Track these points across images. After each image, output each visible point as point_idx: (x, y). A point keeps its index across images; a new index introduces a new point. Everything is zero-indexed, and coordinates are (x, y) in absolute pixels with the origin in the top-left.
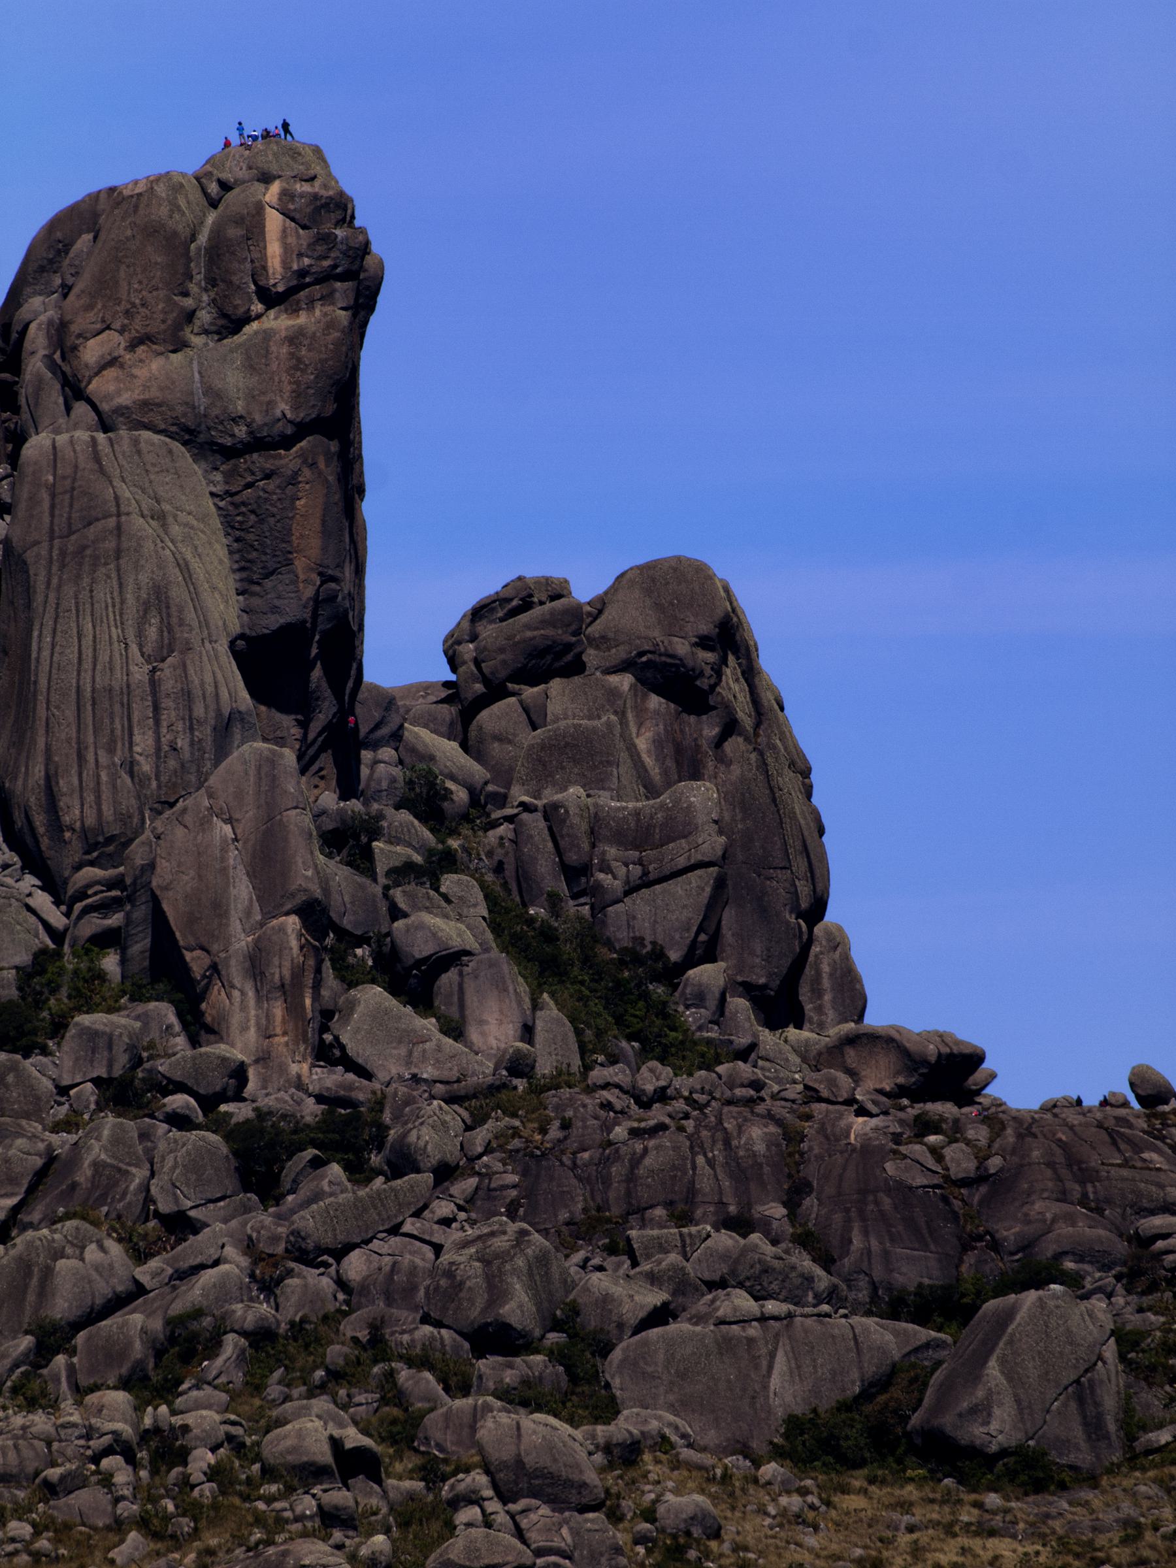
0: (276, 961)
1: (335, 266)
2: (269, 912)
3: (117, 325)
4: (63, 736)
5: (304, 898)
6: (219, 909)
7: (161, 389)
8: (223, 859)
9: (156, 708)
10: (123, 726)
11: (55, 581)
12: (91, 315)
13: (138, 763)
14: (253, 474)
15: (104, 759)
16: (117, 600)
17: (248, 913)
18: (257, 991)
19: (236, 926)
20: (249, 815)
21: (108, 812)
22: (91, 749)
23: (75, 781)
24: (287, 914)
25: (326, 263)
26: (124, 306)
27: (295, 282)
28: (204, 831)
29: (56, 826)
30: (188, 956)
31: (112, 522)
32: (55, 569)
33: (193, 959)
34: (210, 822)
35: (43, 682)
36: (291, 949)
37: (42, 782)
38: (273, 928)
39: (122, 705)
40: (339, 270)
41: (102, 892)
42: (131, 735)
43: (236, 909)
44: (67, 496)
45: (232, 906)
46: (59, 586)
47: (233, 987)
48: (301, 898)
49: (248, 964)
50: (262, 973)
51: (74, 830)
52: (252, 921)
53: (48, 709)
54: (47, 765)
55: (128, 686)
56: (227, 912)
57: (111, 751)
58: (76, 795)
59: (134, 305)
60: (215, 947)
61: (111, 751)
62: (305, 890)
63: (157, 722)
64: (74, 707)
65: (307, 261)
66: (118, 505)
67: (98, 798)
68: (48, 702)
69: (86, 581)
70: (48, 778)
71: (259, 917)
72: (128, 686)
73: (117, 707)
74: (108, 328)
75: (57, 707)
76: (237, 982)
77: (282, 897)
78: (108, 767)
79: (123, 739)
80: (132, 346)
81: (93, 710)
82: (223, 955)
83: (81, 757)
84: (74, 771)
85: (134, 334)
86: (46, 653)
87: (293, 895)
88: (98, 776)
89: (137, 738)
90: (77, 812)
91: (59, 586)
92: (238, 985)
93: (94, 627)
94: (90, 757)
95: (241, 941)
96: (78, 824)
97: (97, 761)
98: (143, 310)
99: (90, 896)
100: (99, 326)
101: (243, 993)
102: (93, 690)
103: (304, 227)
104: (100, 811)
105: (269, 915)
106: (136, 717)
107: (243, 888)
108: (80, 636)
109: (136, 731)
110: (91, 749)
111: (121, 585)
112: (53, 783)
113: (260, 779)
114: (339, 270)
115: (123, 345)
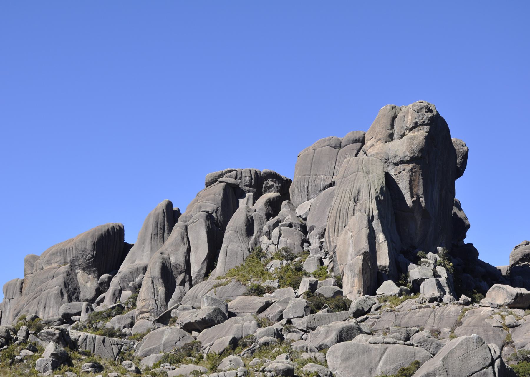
1: (424, 122)
6: (346, 255)
11: (341, 186)
24: (360, 255)
69: (346, 186)
74: (372, 138)
80: (377, 141)
100: (371, 138)
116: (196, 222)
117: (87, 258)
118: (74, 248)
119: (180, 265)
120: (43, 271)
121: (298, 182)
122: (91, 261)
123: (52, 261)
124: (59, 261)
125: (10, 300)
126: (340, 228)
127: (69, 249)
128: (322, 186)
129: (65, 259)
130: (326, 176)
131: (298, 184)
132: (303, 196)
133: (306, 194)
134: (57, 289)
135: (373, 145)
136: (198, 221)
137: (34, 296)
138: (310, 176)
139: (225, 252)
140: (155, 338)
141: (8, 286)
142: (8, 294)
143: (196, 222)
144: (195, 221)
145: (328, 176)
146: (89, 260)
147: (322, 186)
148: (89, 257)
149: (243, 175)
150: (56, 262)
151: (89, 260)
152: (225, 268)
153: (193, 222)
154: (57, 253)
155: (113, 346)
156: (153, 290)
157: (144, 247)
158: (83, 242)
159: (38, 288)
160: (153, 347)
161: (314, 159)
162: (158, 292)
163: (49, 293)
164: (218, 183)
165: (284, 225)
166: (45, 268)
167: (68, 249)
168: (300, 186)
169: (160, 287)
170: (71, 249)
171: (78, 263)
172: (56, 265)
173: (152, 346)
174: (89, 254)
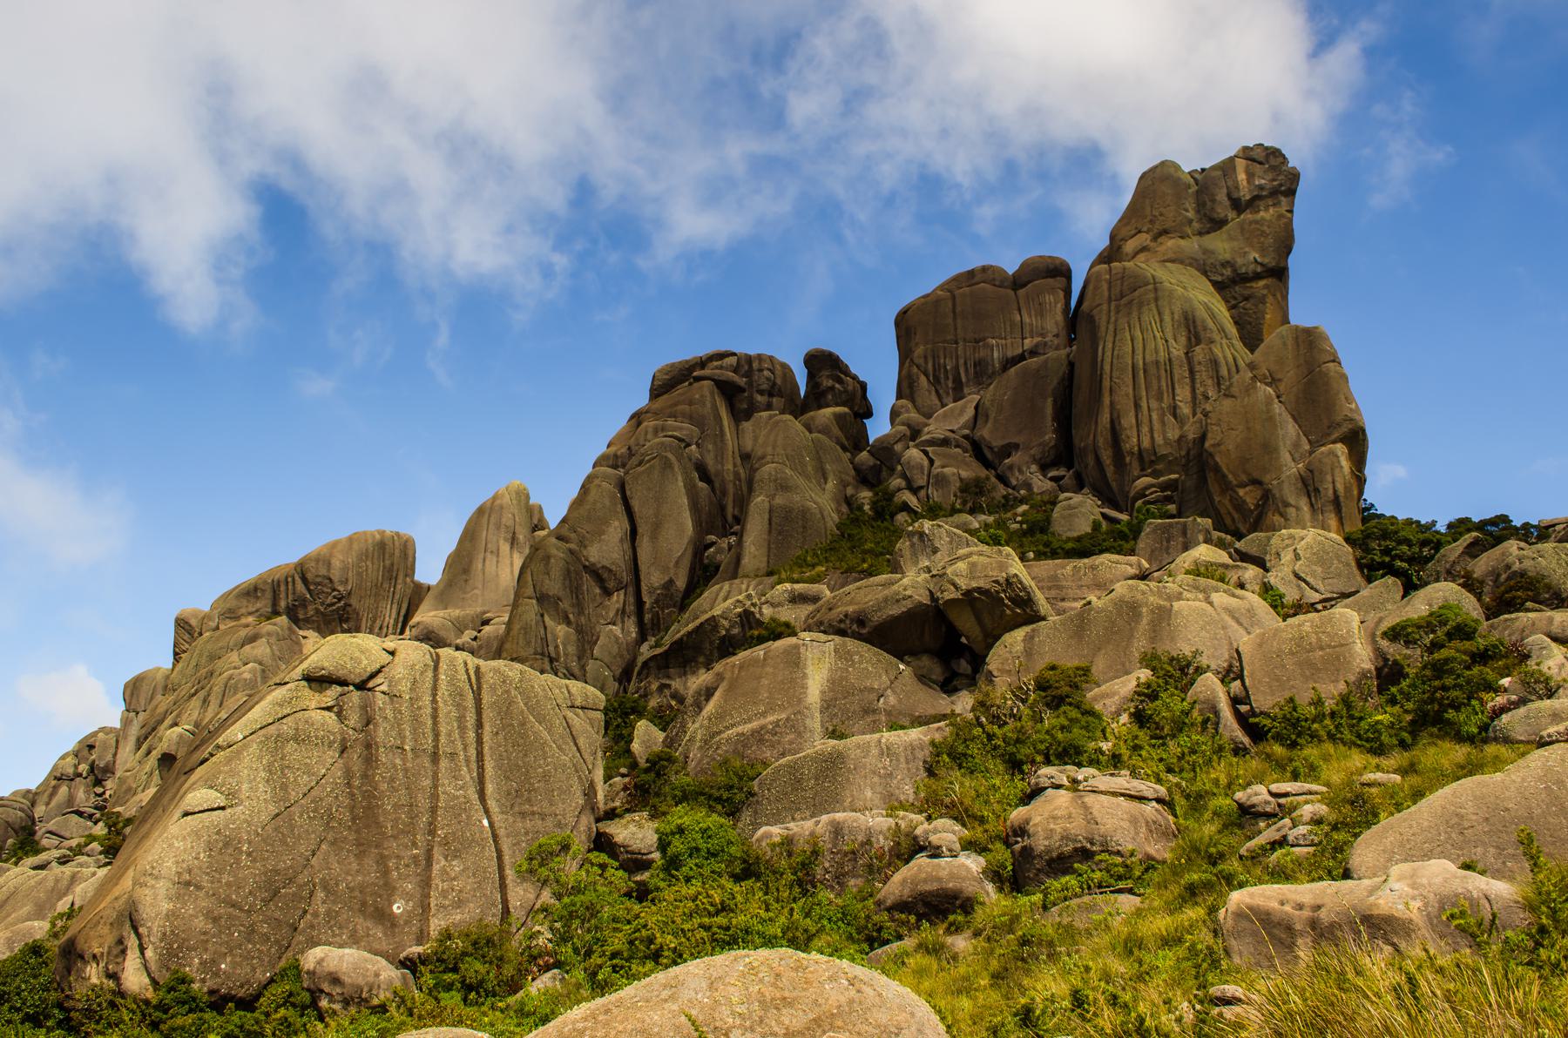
0: (1329, 478)
1: (1281, 185)
2: (1317, 441)
3: (1145, 229)
4: (1123, 393)
5: (1350, 426)
6: (1269, 449)
7: (1175, 253)
8: (1268, 411)
9: (1192, 372)
10: (1167, 386)
11: (1113, 319)
12: (1129, 228)
13: (1180, 408)
14: (1235, 299)
15: (1154, 404)
16: (1158, 320)
17: (1297, 445)
18: (1312, 505)
19: (1286, 457)
20: (1290, 376)
21: (1159, 440)
22: (1144, 399)
23: (1134, 421)
24: (1334, 442)
25: (1275, 183)
26: (1149, 218)
27: (1256, 193)
28: (1249, 395)
29: (1118, 455)
30: (1241, 492)
31: (1151, 287)
32: (1112, 314)
33: (1246, 493)
34: (1255, 388)
35: (1107, 368)
36: (1342, 467)
37: (1108, 426)
38: (1322, 453)
39: (1166, 371)
40: (1283, 188)
41: (1156, 492)
42: (1173, 389)
43: (1285, 444)
44: (1119, 282)
45: (1281, 444)
46: (1116, 321)
47: (1287, 505)
48: (1345, 428)
49: (1300, 485)
50: (1317, 490)
51: (1133, 453)
52: (1301, 450)
53: (1111, 380)
54: (1111, 414)
55: (1170, 360)
56: (1276, 450)
57: (1160, 398)
58: (1135, 429)
59: (1155, 216)
60: (1266, 479)
61: (1160, 398)
62: (1351, 420)
63: (1193, 381)
64: (1131, 376)
65: (1263, 182)
66: (1154, 279)
67: (1151, 430)
68: (1111, 378)
69: (1135, 314)
70: (1112, 421)
71: (1307, 447)
72: (1170, 360)
73: (1163, 372)
74: (1140, 232)
75: (1118, 378)
76: (1292, 501)
77: (1329, 427)
78: (1158, 409)
79: (1168, 392)
80: (1155, 239)
81: (1145, 377)
82: (1275, 482)
83: (1137, 406)
84: (1132, 414)
85: (1156, 231)
86: (1108, 354)
87: (1339, 425)
88: (1150, 416)
89: (1178, 391)
90: (1135, 440)
91: (1116, 321)
92: (1293, 502)
93: (1142, 334)
94: (1144, 404)
95: (1291, 468)
96: (1136, 448)
97: (1149, 407)
98: (1161, 218)
99: (1147, 496)
100: (1133, 232)
101: (1298, 509)
102: (1144, 364)
103: (1261, 163)
104: (1152, 437)
105: (1315, 445)
106: (1176, 377)
107: (1290, 426)
108: (1132, 340)
109: (1177, 386)
110: (1144, 399)
111: (1159, 314)
112: (1117, 424)
113: (1298, 345)
114: (1283, 188)
115: (1149, 238)
116: (649, 461)
117: (328, 601)
118: (297, 578)
119: (610, 571)
120: (217, 633)
121: (926, 357)
122: (338, 608)
123: (243, 611)
124: (257, 611)
125: (137, 713)
126: (1155, 416)
127: (287, 578)
128: (996, 362)
129: (275, 603)
130: (1004, 341)
131: (926, 363)
132: (941, 391)
133: (950, 384)
134: (253, 671)
135: (1144, 249)
136: (655, 458)
137: (193, 690)
138: (956, 343)
139: (766, 516)
140: (765, 682)
141: (135, 684)
142: (134, 701)
143: (649, 461)
144: (647, 458)
145: (1009, 341)
146: (333, 604)
147: (996, 362)
148: (334, 597)
149: (755, 365)
150: (250, 614)
151: (333, 604)
152: (769, 556)
153: (640, 464)
154: (256, 589)
155: (570, 714)
156: (542, 631)
157: (466, 581)
158: (321, 563)
159: (203, 672)
160: (771, 718)
161: (958, 309)
162: (555, 638)
163: (230, 678)
164: (690, 384)
165: (932, 443)
166: (222, 627)
167: (283, 579)
168: (934, 365)
169: (559, 624)
170: (290, 579)
171: (306, 614)
172: (250, 619)
173: (764, 714)
174: (334, 590)
